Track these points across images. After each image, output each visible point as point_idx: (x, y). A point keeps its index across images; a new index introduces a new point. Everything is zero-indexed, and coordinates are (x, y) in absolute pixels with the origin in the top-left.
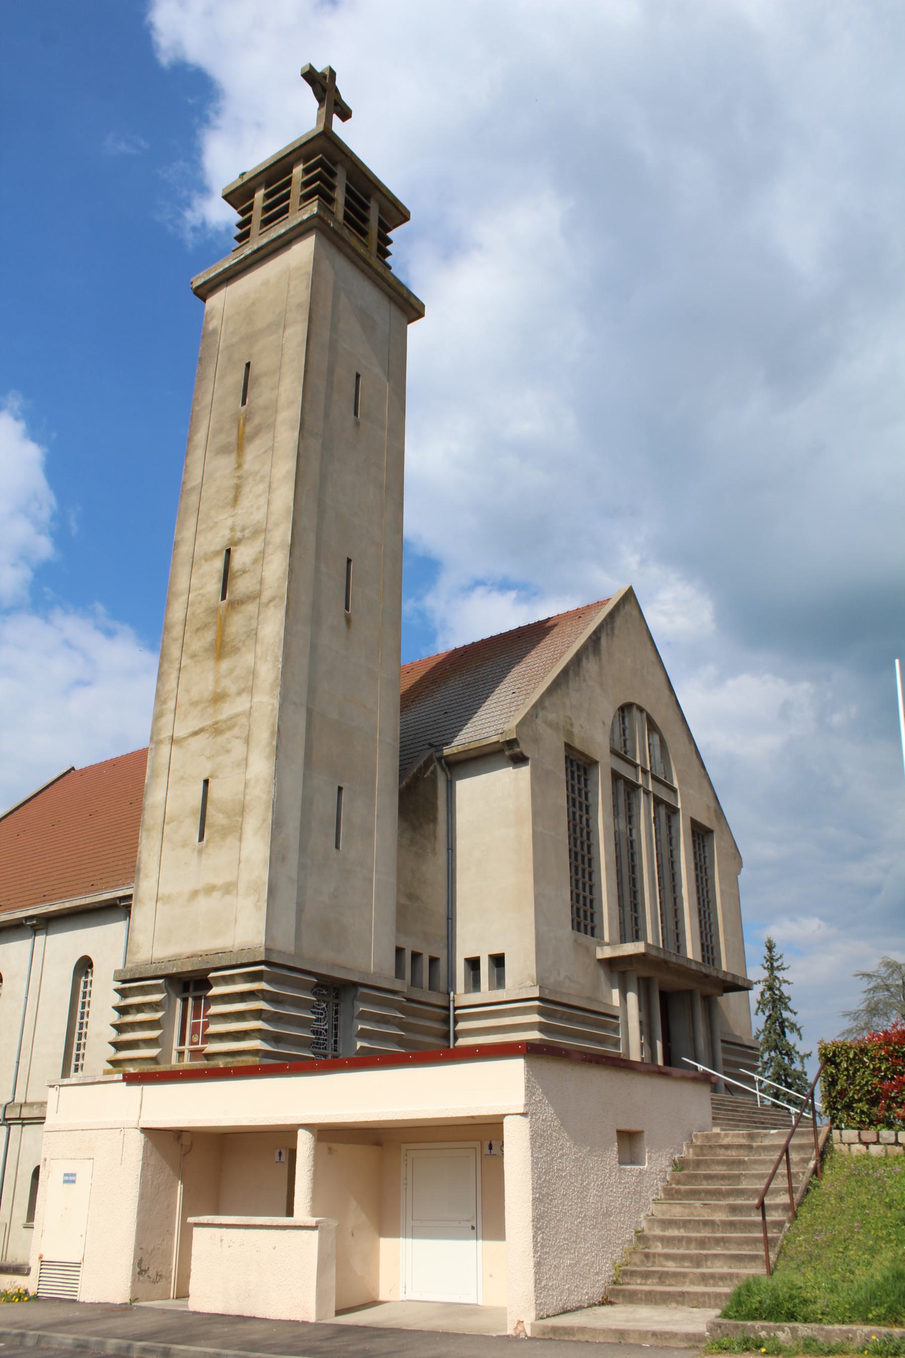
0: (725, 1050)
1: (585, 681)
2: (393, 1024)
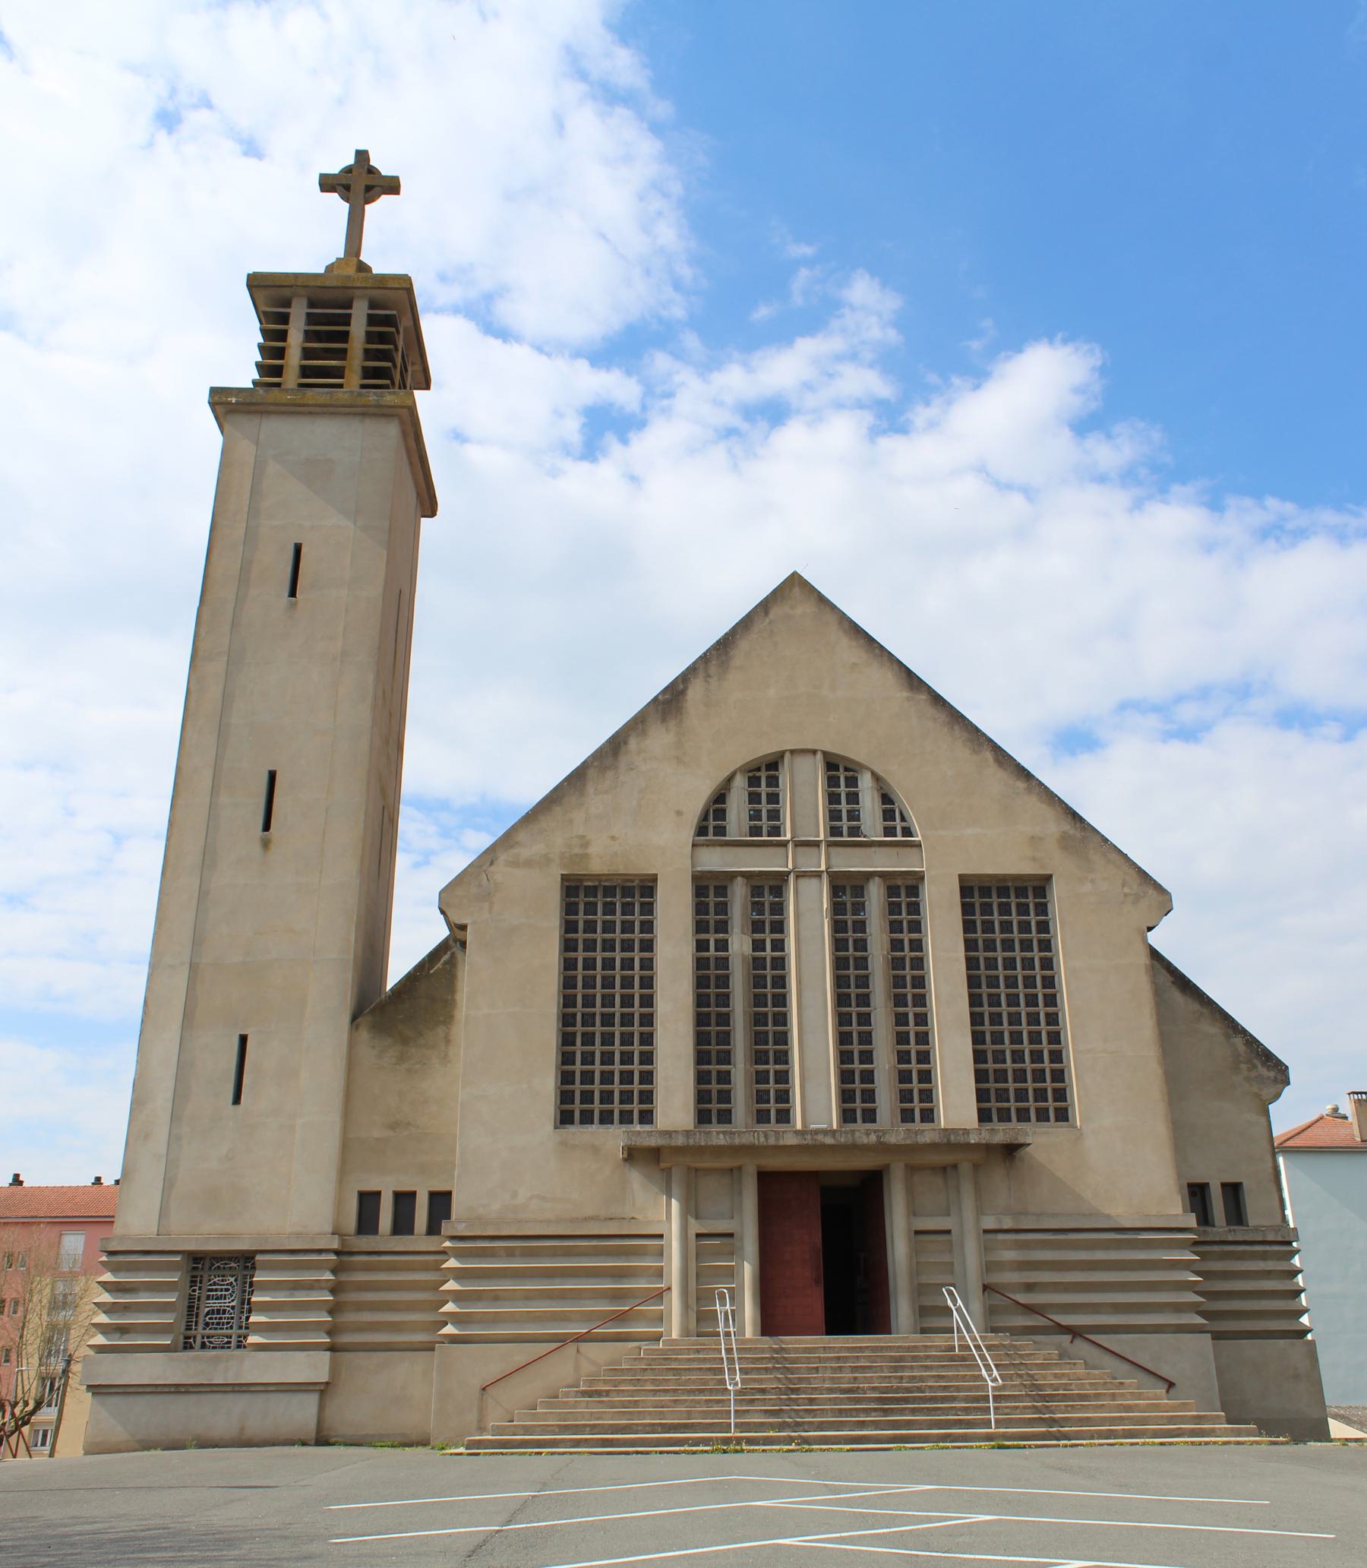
2: (321, 1288)
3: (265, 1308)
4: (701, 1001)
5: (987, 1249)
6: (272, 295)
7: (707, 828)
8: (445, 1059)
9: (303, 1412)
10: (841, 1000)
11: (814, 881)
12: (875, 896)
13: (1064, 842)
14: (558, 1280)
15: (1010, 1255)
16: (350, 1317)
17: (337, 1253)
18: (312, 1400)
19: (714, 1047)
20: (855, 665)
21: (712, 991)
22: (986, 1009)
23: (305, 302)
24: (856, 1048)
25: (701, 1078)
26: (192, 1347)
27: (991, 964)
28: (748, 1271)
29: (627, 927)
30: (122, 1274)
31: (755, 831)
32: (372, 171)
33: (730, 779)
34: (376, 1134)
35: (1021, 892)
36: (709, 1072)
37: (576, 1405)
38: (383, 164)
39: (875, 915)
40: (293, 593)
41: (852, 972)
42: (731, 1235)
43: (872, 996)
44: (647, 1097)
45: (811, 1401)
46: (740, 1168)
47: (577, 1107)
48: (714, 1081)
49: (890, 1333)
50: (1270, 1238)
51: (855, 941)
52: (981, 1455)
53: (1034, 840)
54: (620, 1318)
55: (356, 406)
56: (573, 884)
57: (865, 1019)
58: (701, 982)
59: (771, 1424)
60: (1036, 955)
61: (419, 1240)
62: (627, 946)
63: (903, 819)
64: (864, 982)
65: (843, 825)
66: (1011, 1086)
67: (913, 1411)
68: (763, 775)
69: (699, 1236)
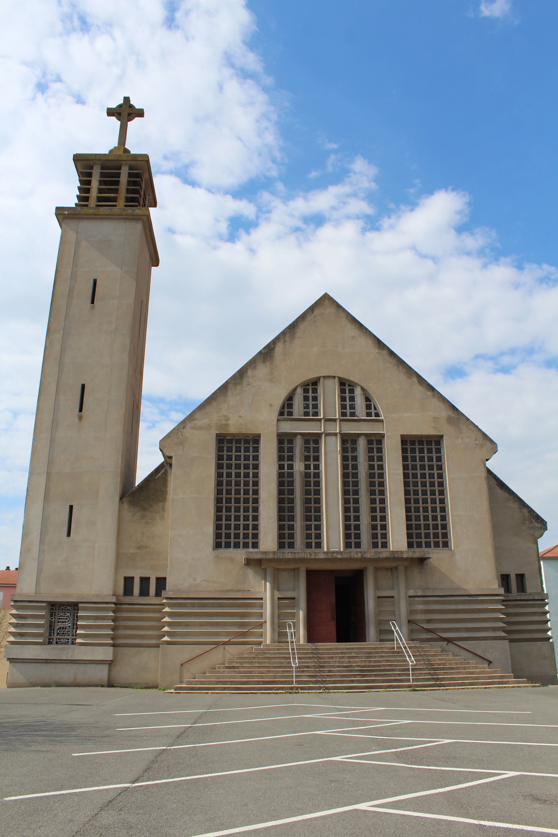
3: (84, 627)
4: (280, 492)
5: (410, 604)
6: (84, 164)
7: (284, 412)
8: (163, 518)
9: (102, 673)
10: (345, 492)
11: (334, 437)
12: (362, 444)
13: (449, 420)
14: (215, 618)
15: (421, 607)
16: (121, 632)
17: (115, 604)
18: (105, 668)
19: (286, 514)
20: (353, 337)
21: (286, 488)
22: (412, 497)
23: (99, 167)
24: (352, 514)
25: (281, 528)
26: (52, 643)
27: (415, 476)
28: (302, 614)
29: (247, 458)
30: (20, 611)
31: (307, 414)
32: (131, 106)
33: (295, 390)
34: (132, 551)
35: (429, 443)
36: (284, 525)
37: (224, 672)
38: (136, 103)
39: (362, 453)
40: (93, 302)
41: (351, 479)
42: (294, 598)
43: (359, 491)
44: (256, 536)
45: (330, 671)
46: (298, 569)
47: (223, 540)
48: (286, 529)
49: (365, 641)
50: (536, 598)
51: (352, 465)
52: (405, 694)
53: (436, 419)
54: (243, 634)
55: (123, 215)
56: (222, 438)
57: (356, 501)
58: (281, 484)
59: (311, 681)
60: (435, 472)
61: (152, 599)
62: (247, 467)
63: (375, 409)
64: (356, 484)
65: (347, 412)
66: (423, 531)
67: (376, 675)
68: (310, 388)
69: (279, 599)
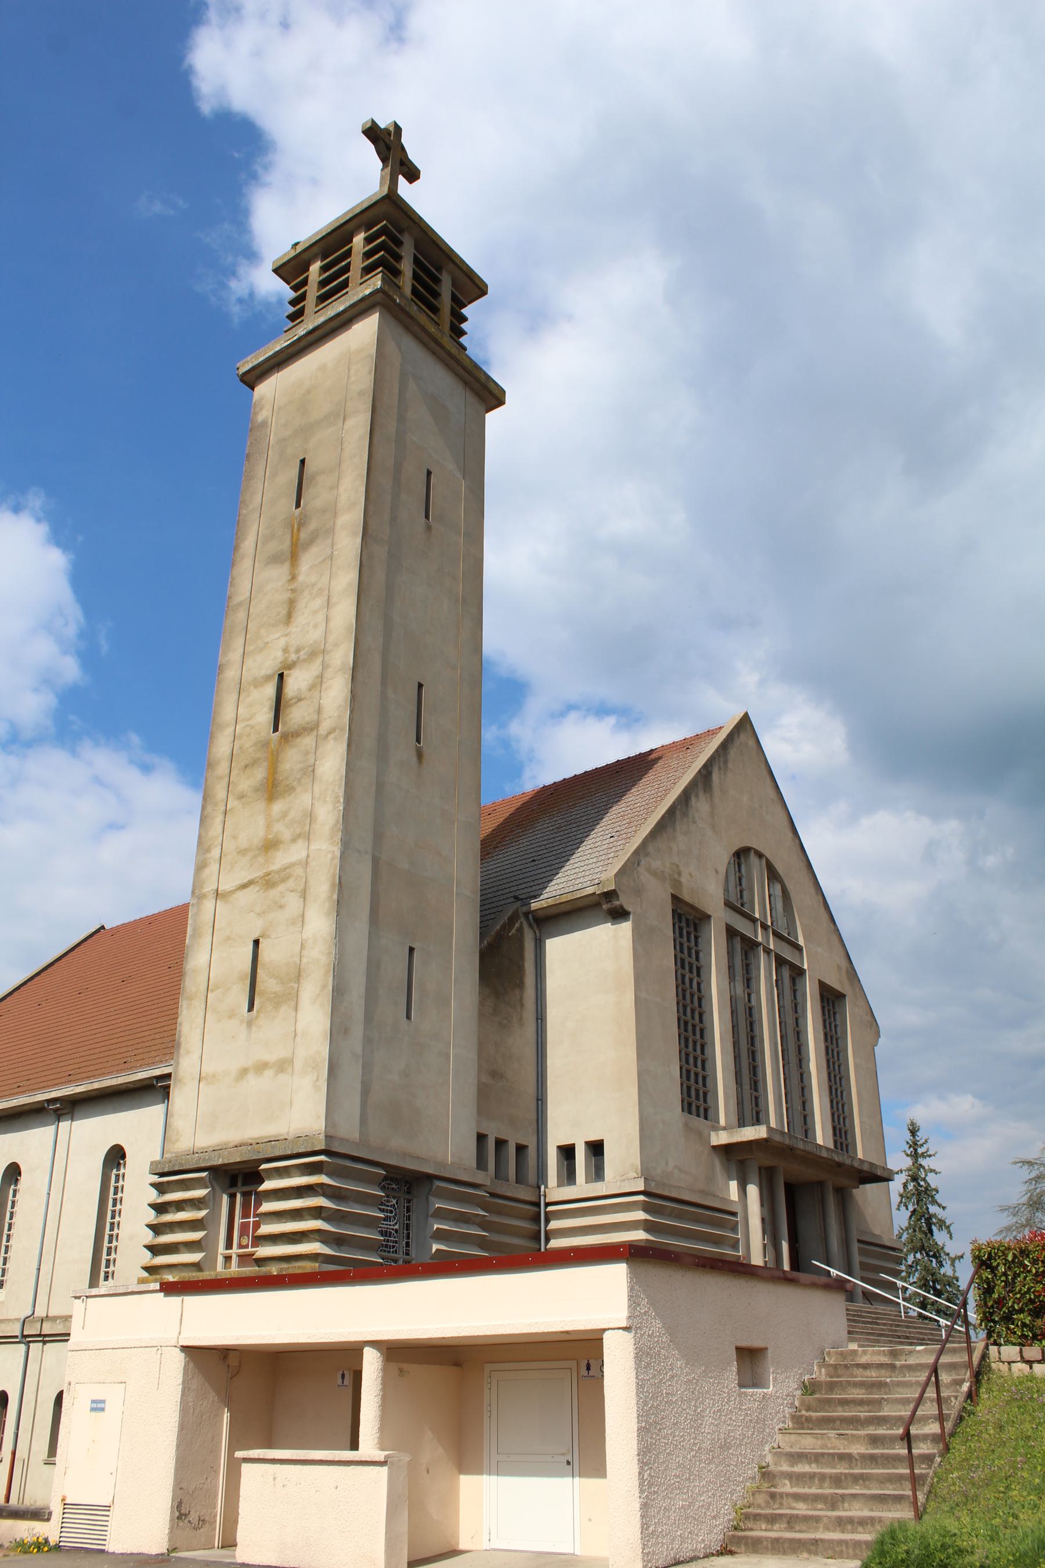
0: (862, 1252)
1: (694, 822)
2: (474, 1223)
